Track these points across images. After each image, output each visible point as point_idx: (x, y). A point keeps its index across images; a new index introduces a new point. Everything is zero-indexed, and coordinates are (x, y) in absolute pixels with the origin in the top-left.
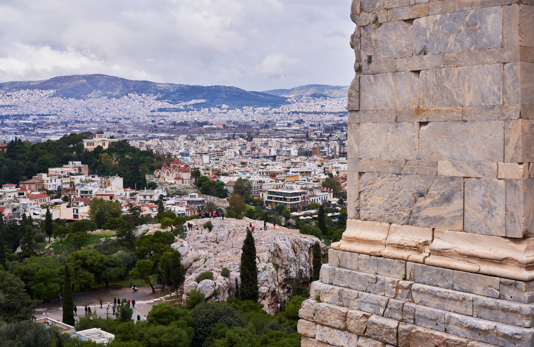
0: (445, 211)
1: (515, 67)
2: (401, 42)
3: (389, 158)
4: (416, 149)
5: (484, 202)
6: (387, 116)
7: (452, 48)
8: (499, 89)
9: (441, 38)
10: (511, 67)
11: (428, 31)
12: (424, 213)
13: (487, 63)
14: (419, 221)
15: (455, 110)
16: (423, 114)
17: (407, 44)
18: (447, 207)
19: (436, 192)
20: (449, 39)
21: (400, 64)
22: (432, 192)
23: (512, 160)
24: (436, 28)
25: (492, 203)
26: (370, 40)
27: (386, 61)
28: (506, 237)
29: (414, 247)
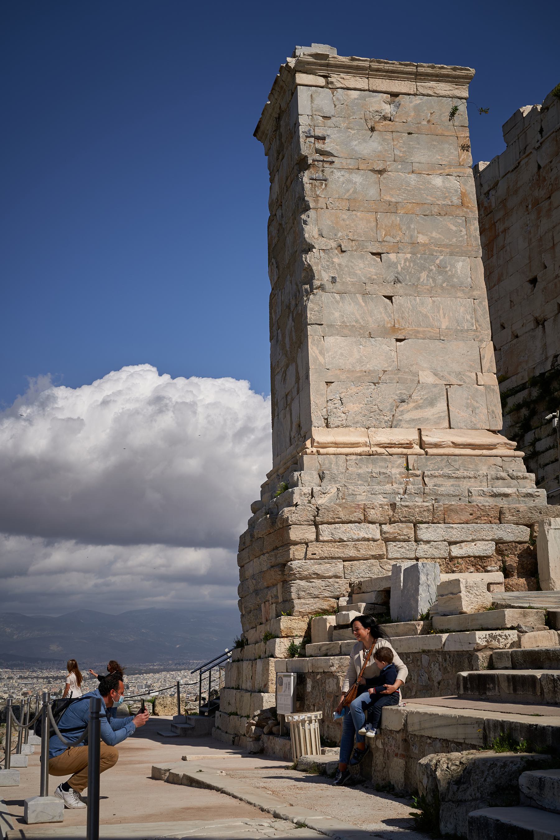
1: (484, 303)
2: (369, 270)
3: (364, 369)
4: (394, 361)
5: (467, 403)
6: (359, 331)
7: (425, 282)
8: (471, 317)
9: (413, 272)
10: (481, 303)
11: (399, 265)
12: (407, 416)
13: (459, 297)
15: (432, 331)
16: (400, 332)
17: (376, 272)
21: (369, 288)
22: (414, 397)
23: (489, 371)
24: (408, 264)
25: (475, 404)
26: (333, 263)
27: (353, 284)
28: (488, 430)
29: (407, 444)
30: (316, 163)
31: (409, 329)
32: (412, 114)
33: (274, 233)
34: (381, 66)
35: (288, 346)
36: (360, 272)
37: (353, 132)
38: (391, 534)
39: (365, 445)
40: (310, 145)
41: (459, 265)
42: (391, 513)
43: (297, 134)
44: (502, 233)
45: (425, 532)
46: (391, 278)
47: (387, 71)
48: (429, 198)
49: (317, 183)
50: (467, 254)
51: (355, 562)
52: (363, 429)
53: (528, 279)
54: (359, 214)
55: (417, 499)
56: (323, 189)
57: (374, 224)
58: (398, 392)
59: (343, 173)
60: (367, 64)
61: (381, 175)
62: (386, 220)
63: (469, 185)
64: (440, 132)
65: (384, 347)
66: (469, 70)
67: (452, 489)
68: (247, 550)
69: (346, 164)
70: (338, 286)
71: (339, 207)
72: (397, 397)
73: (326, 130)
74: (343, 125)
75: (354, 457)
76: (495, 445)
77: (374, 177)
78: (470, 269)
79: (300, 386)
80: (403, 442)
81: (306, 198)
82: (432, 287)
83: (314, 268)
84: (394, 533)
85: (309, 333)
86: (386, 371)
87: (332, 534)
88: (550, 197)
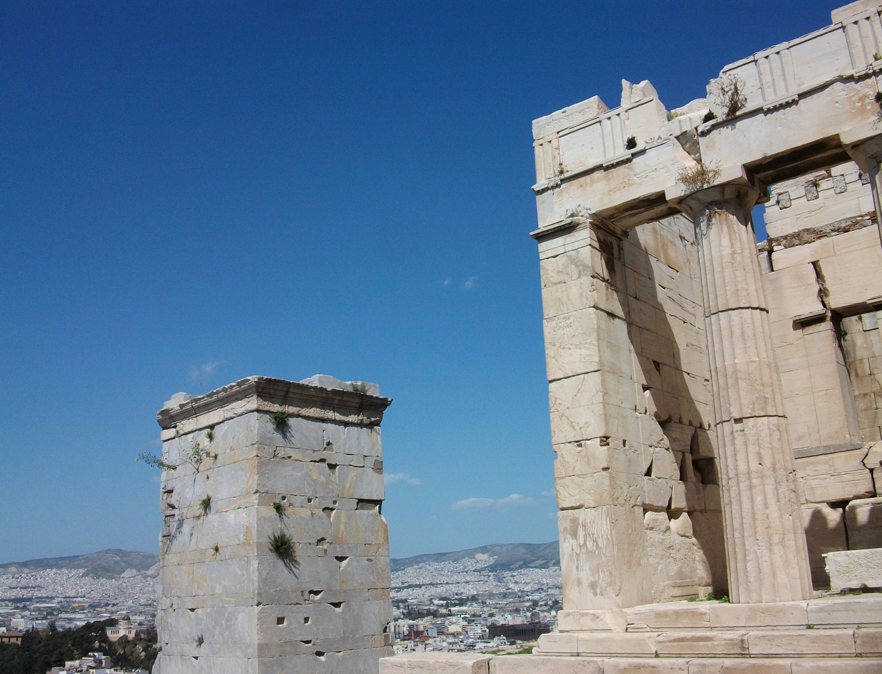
10: (252, 663)
26: (168, 623)
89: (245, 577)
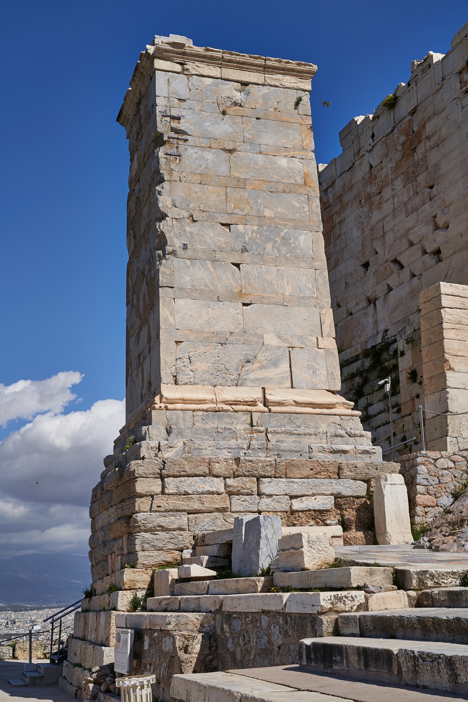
0: (272, 373)
1: (324, 273)
3: (212, 330)
4: (240, 324)
6: (208, 295)
7: (270, 252)
8: (313, 286)
9: (259, 243)
10: (321, 273)
11: (246, 235)
12: (252, 376)
14: (248, 382)
16: (246, 297)
17: (225, 241)
18: (275, 370)
19: (264, 359)
20: (267, 245)
21: (218, 255)
22: (259, 357)
23: (328, 336)
24: (254, 235)
25: (316, 366)
26: (185, 231)
27: (204, 251)
28: (328, 391)
29: (252, 402)
30: (171, 140)
31: (254, 294)
32: (261, 101)
33: (133, 206)
34: (233, 57)
35: (141, 309)
36: (210, 241)
37: (206, 114)
38: (235, 487)
39: (212, 402)
40: (166, 124)
41: (302, 238)
42: (235, 467)
43: (154, 113)
44: (339, 223)
45: (268, 486)
46: (239, 247)
47: (238, 63)
48: (275, 176)
49: (172, 158)
50: (309, 229)
51: (200, 515)
52: (210, 387)
53: (361, 264)
54: (210, 188)
55: (260, 454)
56: (177, 164)
57: (224, 197)
58: (244, 353)
59: (196, 150)
60: (219, 55)
61: (231, 154)
62: (235, 194)
63: (311, 167)
64: (285, 119)
65: (232, 310)
66: (312, 66)
67: (294, 445)
68: (98, 502)
69: (199, 142)
70: (189, 253)
71: (191, 180)
72: (242, 358)
73: (181, 111)
74: (197, 108)
75: (200, 413)
76: (334, 405)
77: (226, 155)
78: (311, 242)
79: (152, 346)
80: (247, 400)
81: (161, 171)
82: (277, 257)
83: (167, 235)
84: (238, 487)
85: (160, 295)
86: (233, 333)
87: (178, 487)
88: (380, 193)
89: (305, 210)
